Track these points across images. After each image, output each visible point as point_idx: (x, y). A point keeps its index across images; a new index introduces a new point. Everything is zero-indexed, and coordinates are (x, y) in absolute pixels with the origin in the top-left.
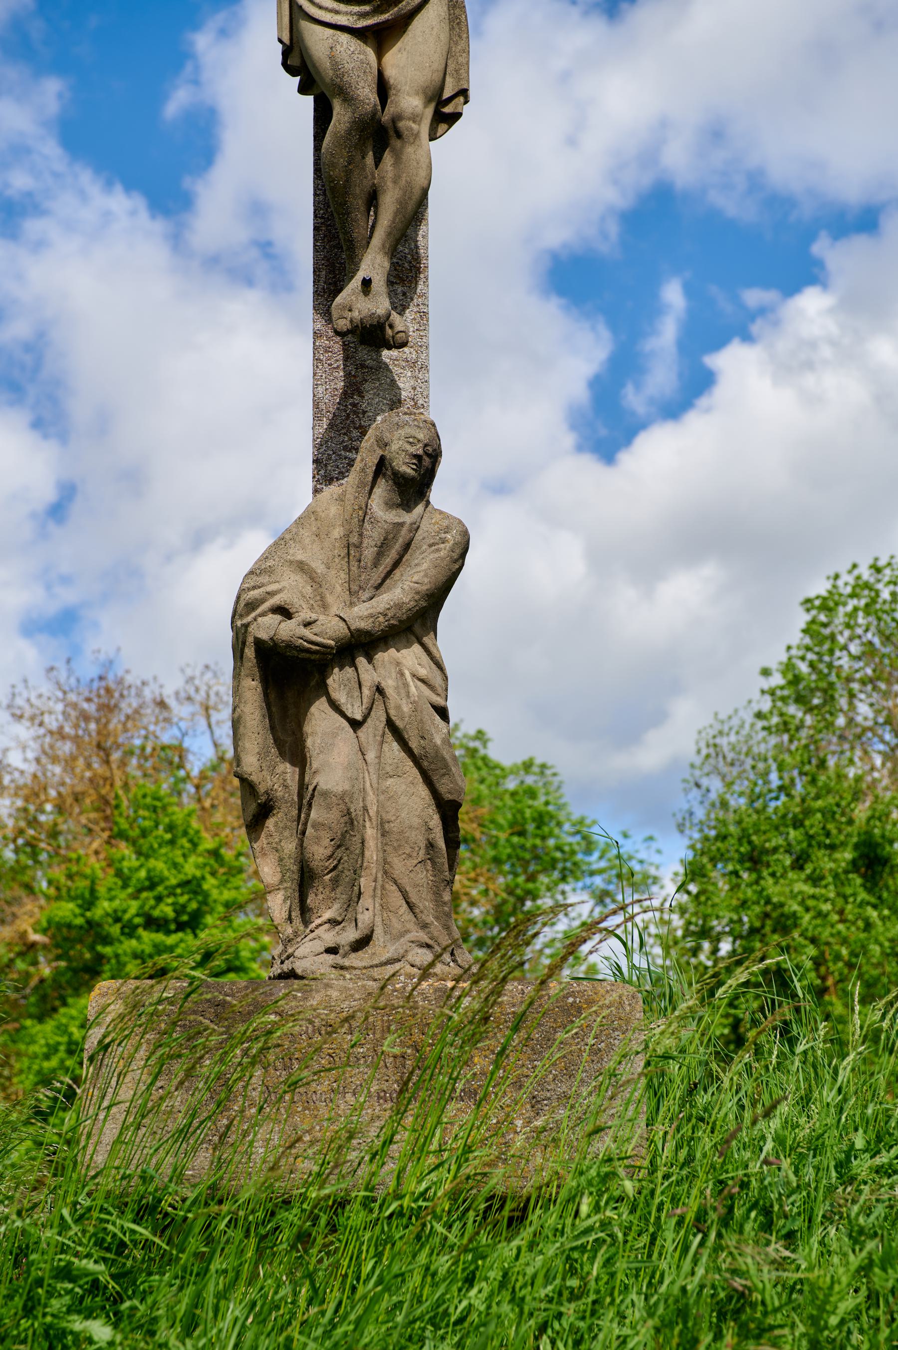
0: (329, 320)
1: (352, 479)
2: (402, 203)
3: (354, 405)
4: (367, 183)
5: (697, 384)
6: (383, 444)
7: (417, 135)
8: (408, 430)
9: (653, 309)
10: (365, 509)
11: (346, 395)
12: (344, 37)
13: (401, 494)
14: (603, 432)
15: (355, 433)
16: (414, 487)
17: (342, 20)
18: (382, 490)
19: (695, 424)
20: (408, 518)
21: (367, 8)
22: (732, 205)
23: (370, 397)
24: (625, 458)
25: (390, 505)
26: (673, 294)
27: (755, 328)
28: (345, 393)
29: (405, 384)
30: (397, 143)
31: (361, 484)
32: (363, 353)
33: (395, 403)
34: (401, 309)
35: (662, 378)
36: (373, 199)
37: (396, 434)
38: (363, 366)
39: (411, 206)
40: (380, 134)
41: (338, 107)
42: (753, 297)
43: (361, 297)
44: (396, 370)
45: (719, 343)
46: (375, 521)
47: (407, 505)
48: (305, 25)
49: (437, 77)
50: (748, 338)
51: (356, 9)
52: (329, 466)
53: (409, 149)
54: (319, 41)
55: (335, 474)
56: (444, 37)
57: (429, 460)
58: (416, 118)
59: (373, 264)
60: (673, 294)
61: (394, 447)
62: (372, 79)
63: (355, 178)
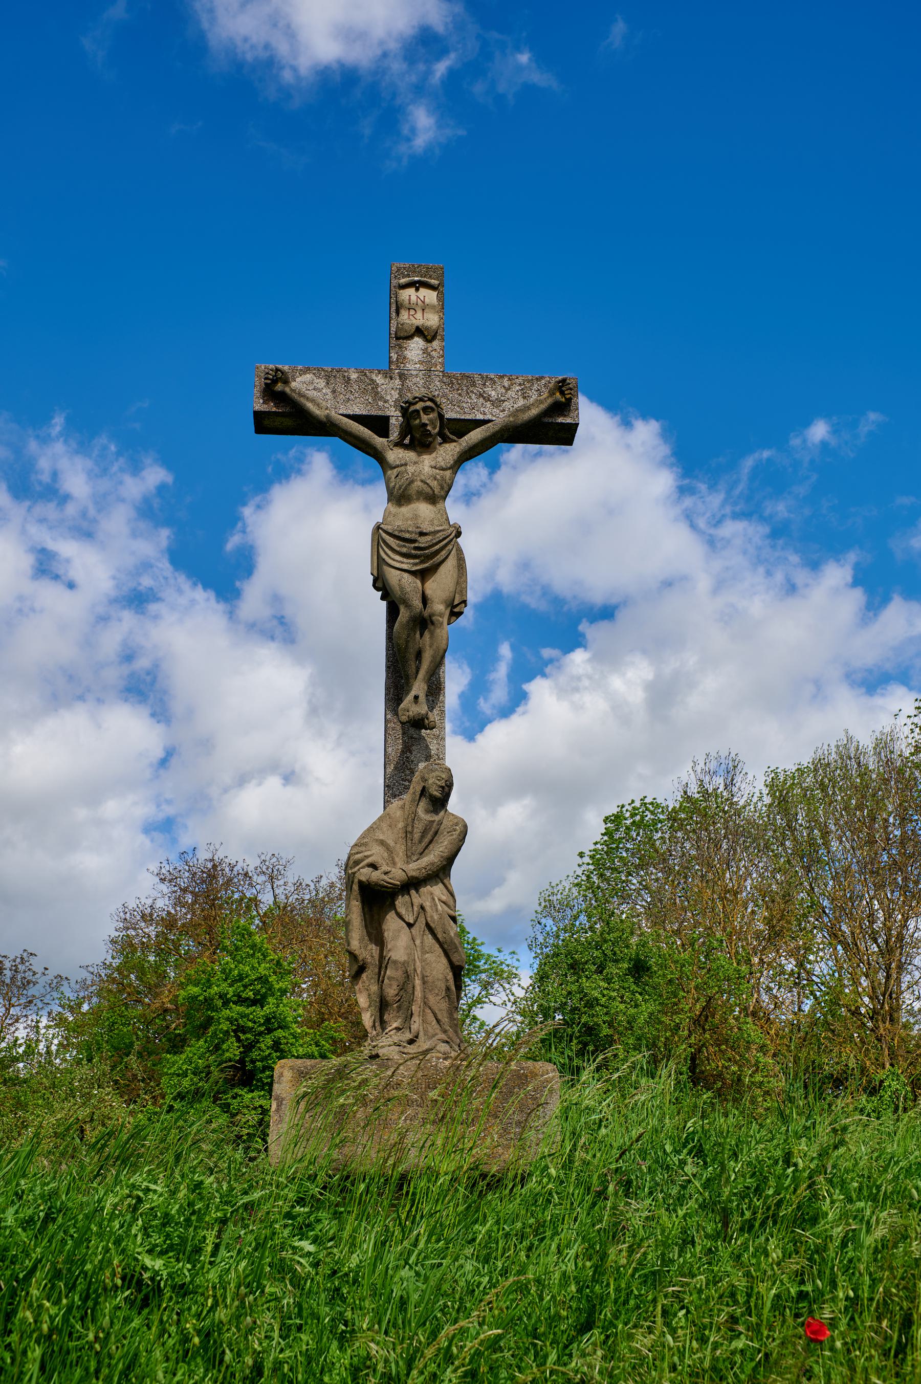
0: (396, 713)
1: (406, 797)
2: (434, 657)
3: (407, 758)
4: (417, 647)
5: (517, 699)
6: (424, 780)
7: (442, 624)
8: (437, 773)
9: (496, 658)
10: (415, 813)
11: (403, 752)
12: (406, 575)
13: (433, 806)
14: (467, 724)
15: (408, 772)
16: (439, 802)
17: (405, 567)
18: (423, 804)
19: (515, 719)
20: (436, 818)
21: (417, 561)
22: (533, 602)
23: (416, 754)
24: (479, 737)
25: (427, 811)
26: (505, 650)
27: (548, 670)
28: (402, 751)
29: (433, 747)
30: (432, 627)
31: (413, 801)
32: (412, 731)
33: (428, 757)
34: (431, 709)
35: (499, 694)
36: (419, 655)
37: (431, 775)
38: (412, 738)
39: (438, 659)
40: (423, 623)
41: (402, 609)
42: (547, 653)
43: (414, 705)
44: (428, 740)
45: (530, 678)
46: (420, 819)
47: (436, 812)
48: (385, 568)
49: (452, 595)
50: (544, 675)
51: (412, 561)
52: (392, 789)
53: (438, 631)
54: (393, 577)
55: (397, 793)
56: (455, 575)
57: (447, 788)
58: (441, 615)
59: (419, 687)
60: (505, 650)
61: (430, 781)
62: (419, 595)
63: (411, 645)
